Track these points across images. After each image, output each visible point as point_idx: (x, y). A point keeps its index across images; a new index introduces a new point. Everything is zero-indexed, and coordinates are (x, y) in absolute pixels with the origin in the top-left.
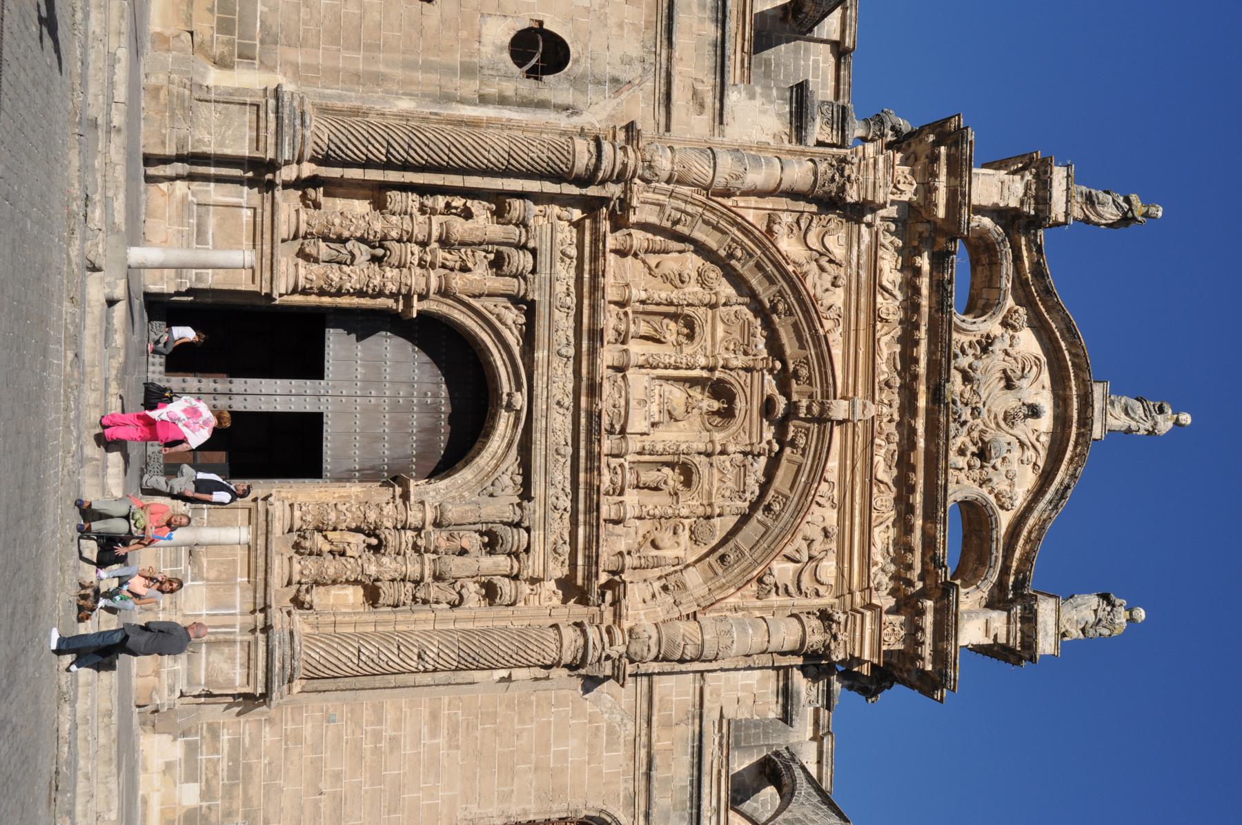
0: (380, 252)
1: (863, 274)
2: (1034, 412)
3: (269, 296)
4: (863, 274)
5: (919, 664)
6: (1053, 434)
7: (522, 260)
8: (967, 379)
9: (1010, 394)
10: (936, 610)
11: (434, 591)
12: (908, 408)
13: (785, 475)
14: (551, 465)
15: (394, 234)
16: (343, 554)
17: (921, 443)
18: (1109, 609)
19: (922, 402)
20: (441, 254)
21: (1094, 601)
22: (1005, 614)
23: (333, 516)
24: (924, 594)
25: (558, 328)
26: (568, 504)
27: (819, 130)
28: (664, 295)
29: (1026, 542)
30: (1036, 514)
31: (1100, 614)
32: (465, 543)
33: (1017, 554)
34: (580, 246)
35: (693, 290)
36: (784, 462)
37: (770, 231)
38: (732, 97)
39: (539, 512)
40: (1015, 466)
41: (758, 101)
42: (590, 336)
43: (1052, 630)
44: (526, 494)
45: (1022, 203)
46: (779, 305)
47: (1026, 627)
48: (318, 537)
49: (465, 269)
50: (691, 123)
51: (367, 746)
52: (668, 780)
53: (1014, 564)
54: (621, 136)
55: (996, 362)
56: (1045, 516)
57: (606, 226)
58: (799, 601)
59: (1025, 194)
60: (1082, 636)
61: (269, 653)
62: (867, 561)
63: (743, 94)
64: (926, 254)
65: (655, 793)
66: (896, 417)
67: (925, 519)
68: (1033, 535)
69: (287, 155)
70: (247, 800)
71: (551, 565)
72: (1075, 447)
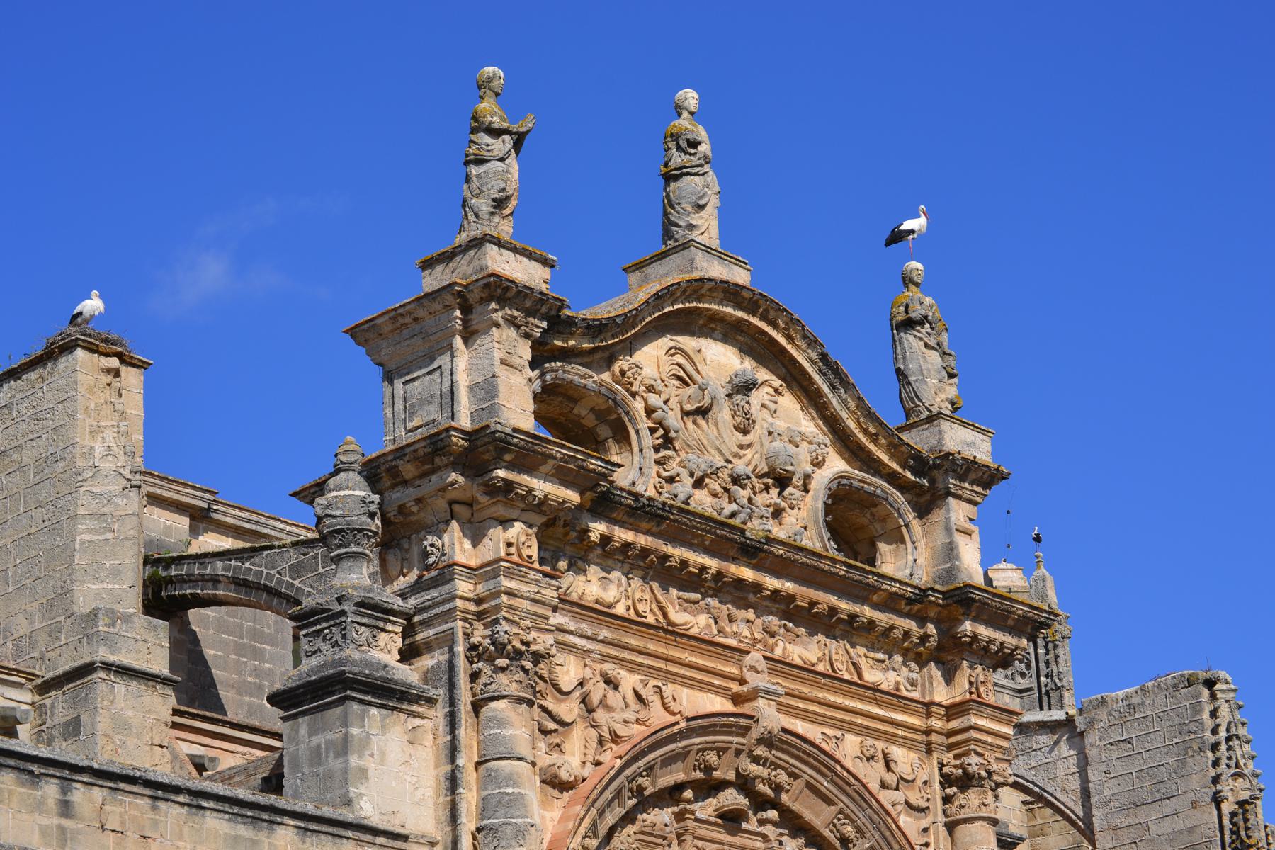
1: (604, 633)
4: (604, 633)
6: (746, 350)
8: (699, 484)
10: (976, 619)
13: (810, 808)
17: (789, 586)
18: (927, 326)
19: (748, 574)
21: (911, 341)
22: (950, 499)
24: (947, 625)
29: (875, 440)
31: (932, 342)
33: (885, 458)
36: (795, 807)
41: (371, 765)
45: (527, 336)
47: (972, 476)
53: (895, 466)
56: (852, 404)
59: (518, 327)
60: (955, 380)
62: (894, 698)
63: (362, 790)
64: (591, 525)
66: (750, 614)
67: (863, 600)
68: (872, 429)
72: (774, 324)
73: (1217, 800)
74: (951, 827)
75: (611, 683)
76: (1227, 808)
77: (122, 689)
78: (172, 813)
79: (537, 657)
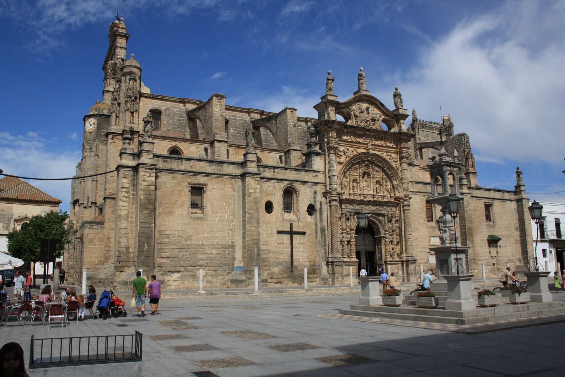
2: (367, 109)
8: (361, 122)
41: (315, 163)
42: (361, 202)
44: (383, 215)
51: (417, 243)
52: (421, 189)
62: (392, 148)
73: (464, 152)
74: (401, 164)
75: (348, 150)
76: (466, 153)
77: (294, 152)
78: (288, 171)
79: (336, 148)
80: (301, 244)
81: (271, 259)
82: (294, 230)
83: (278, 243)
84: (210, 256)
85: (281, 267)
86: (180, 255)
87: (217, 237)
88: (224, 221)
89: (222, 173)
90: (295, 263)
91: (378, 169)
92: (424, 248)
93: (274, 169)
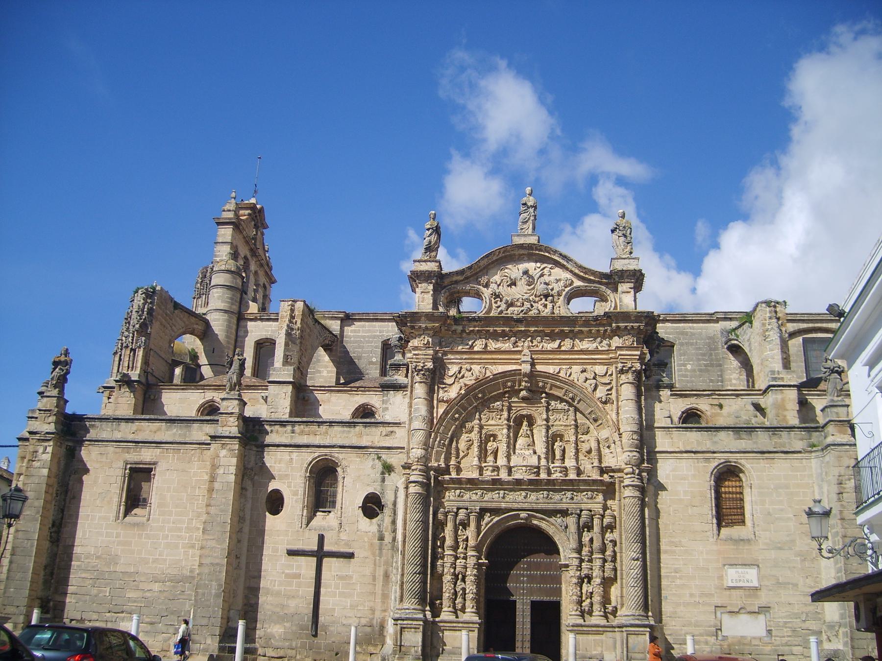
0: (460, 576)
3: (479, 624)
5: (642, 328)
7: (462, 514)
9: (518, 283)
11: (609, 553)
12: (525, 335)
14: (552, 501)
15: (452, 570)
16: (592, 593)
20: (460, 550)
23: (575, 597)
25: (493, 498)
26: (570, 493)
27: (400, 378)
28: (476, 450)
30: (573, 269)
32: (588, 539)
33: (592, 278)
34: (456, 489)
35: (474, 436)
37: (447, 402)
38: (388, 418)
39: (574, 506)
40: (552, 278)
42: (496, 484)
43: (627, 261)
44: (565, 513)
46: (480, 397)
48: (584, 604)
49: (467, 540)
50: (400, 437)
51: (678, 582)
52: (698, 443)
54: (407, 471)
55: (504, 290)
57: (447, 477)
58: (614, 383)
61: (632, 626)
62: (596, 352)
65: (704, 449)
69: (421, 616)
70: (701, 635)
71: (597, 500)
80: (341, 578)
81: (268, 607)
82: (327, 548)
83: (288, 576)
84: (148, 594)
85: (288, 625)
86: (94, 591)
87: (165, 560)
88: (180, 529)
89: (188, 440)
90: (322, 619)
91: (560, 406)
92: (702, 595)
93: (293, 426)
